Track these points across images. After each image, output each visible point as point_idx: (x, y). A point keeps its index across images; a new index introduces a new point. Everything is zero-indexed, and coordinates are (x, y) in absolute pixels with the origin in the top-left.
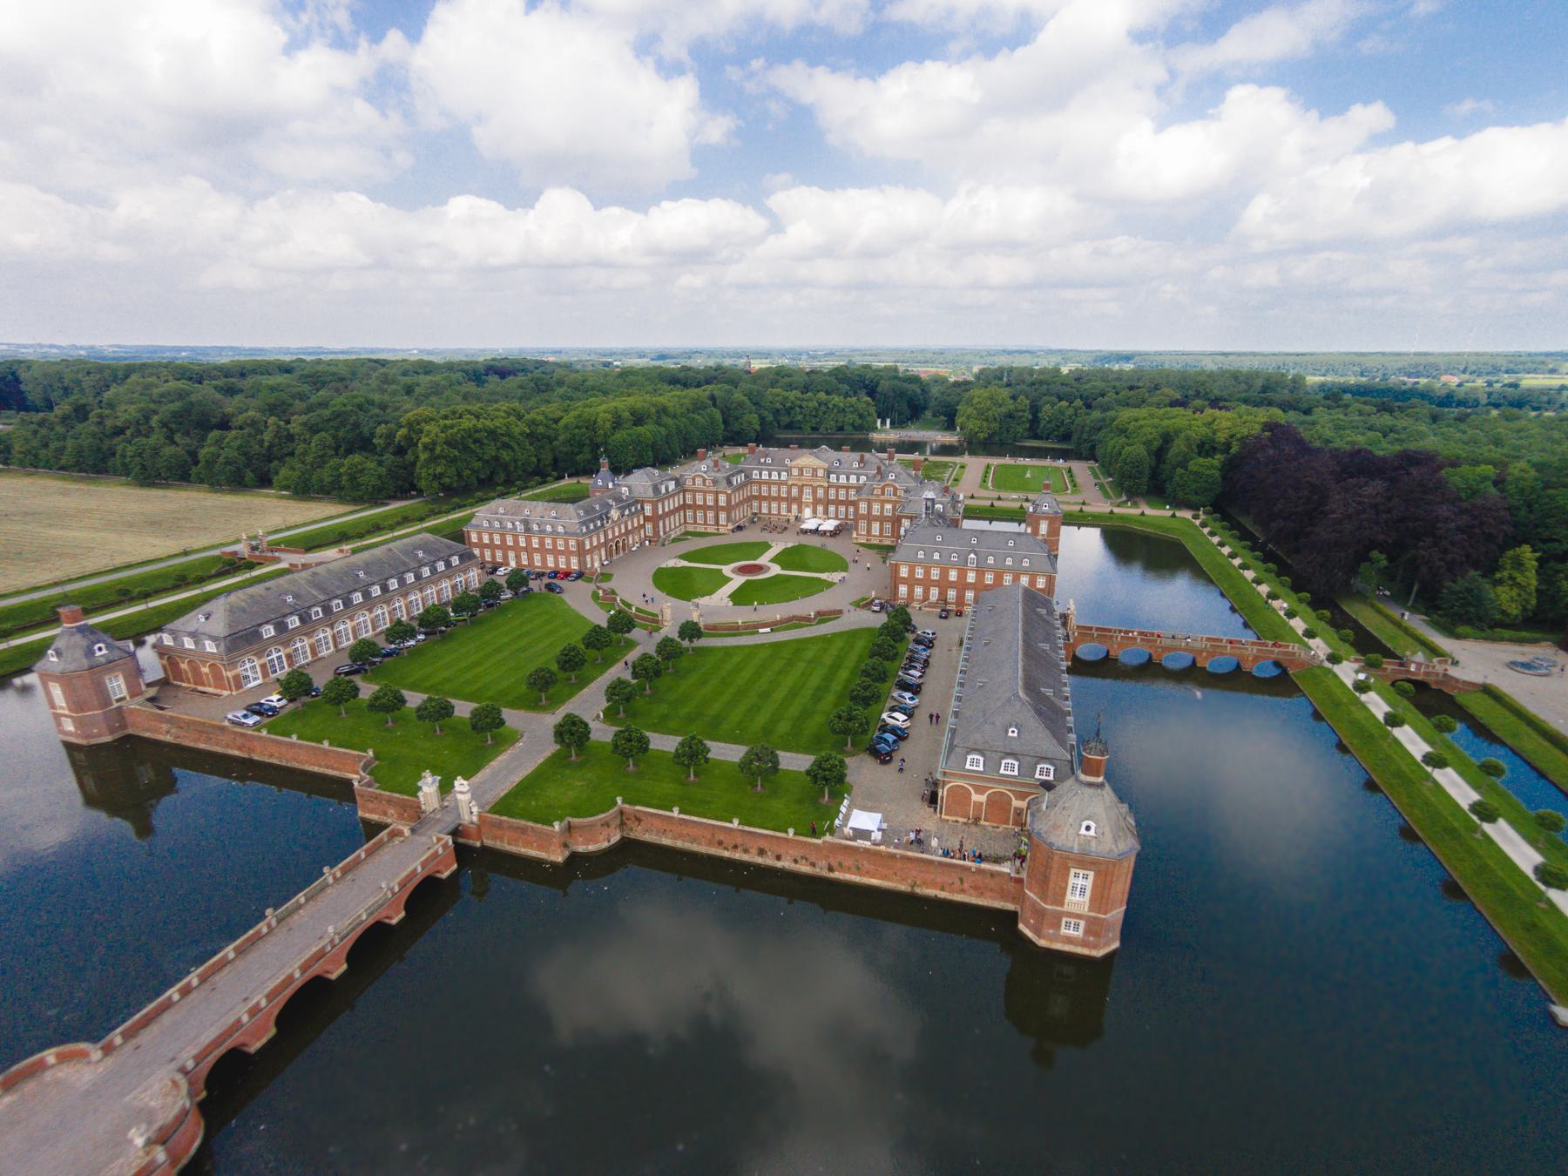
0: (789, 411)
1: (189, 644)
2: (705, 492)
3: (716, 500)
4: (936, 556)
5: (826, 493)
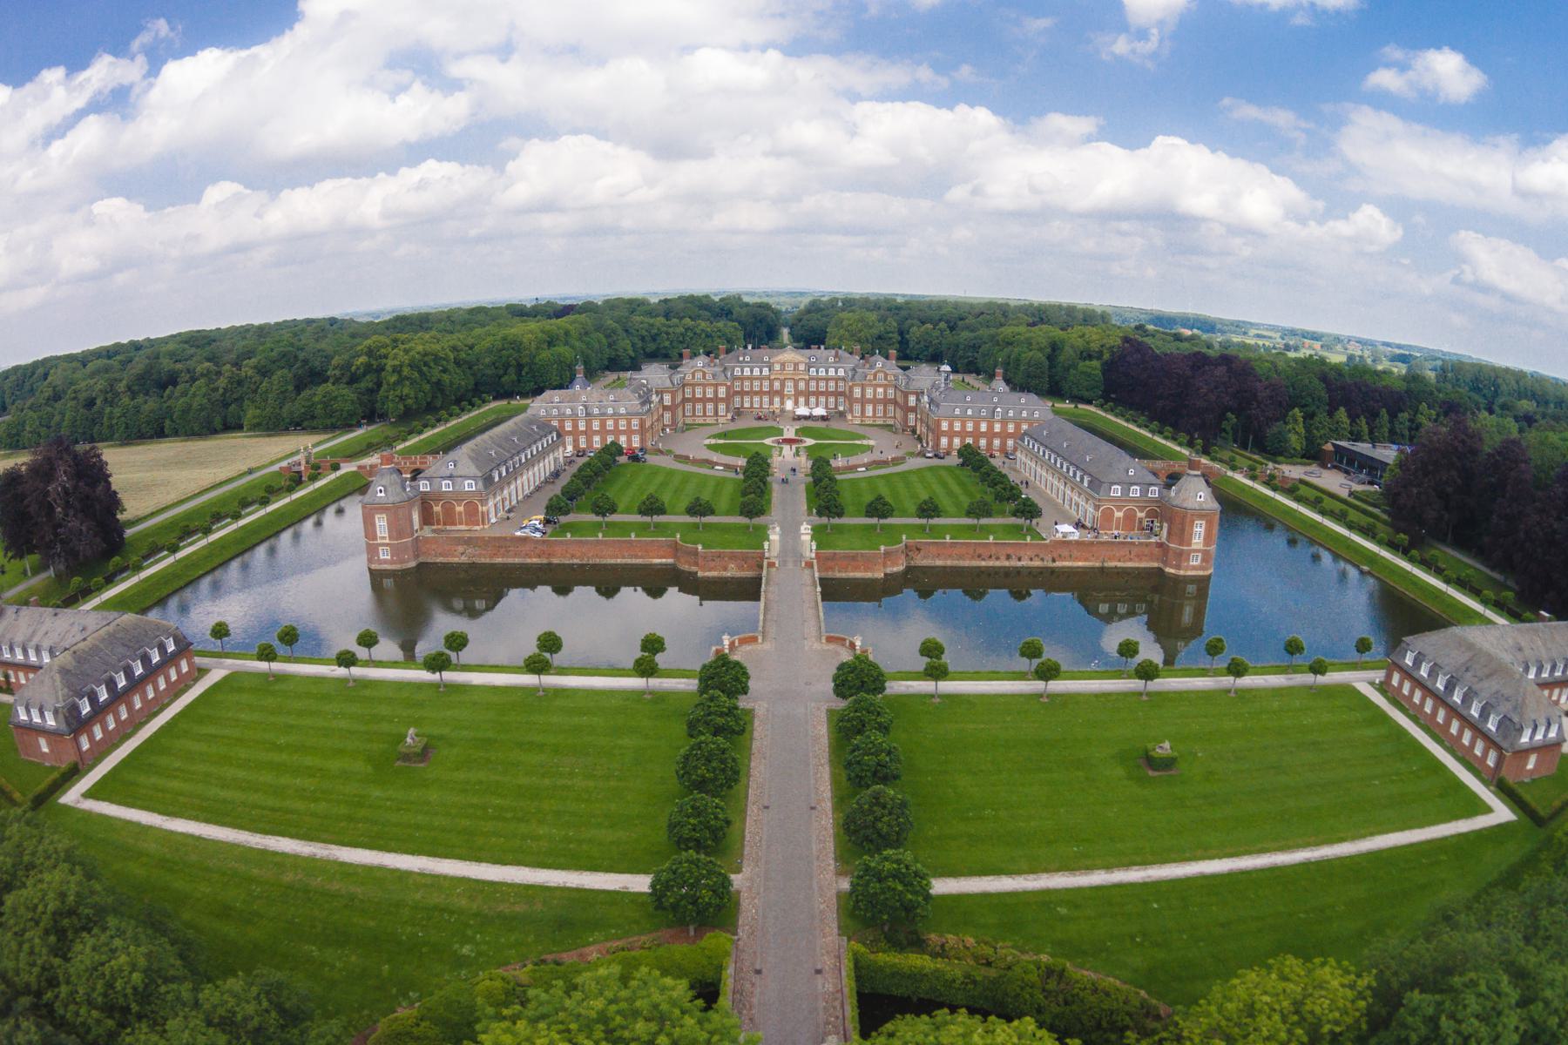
0: (654, 339)
1: (446, 486)
2: (704, 386)
3: (716, 392)
4: (970, 412)
5: (807, 385)
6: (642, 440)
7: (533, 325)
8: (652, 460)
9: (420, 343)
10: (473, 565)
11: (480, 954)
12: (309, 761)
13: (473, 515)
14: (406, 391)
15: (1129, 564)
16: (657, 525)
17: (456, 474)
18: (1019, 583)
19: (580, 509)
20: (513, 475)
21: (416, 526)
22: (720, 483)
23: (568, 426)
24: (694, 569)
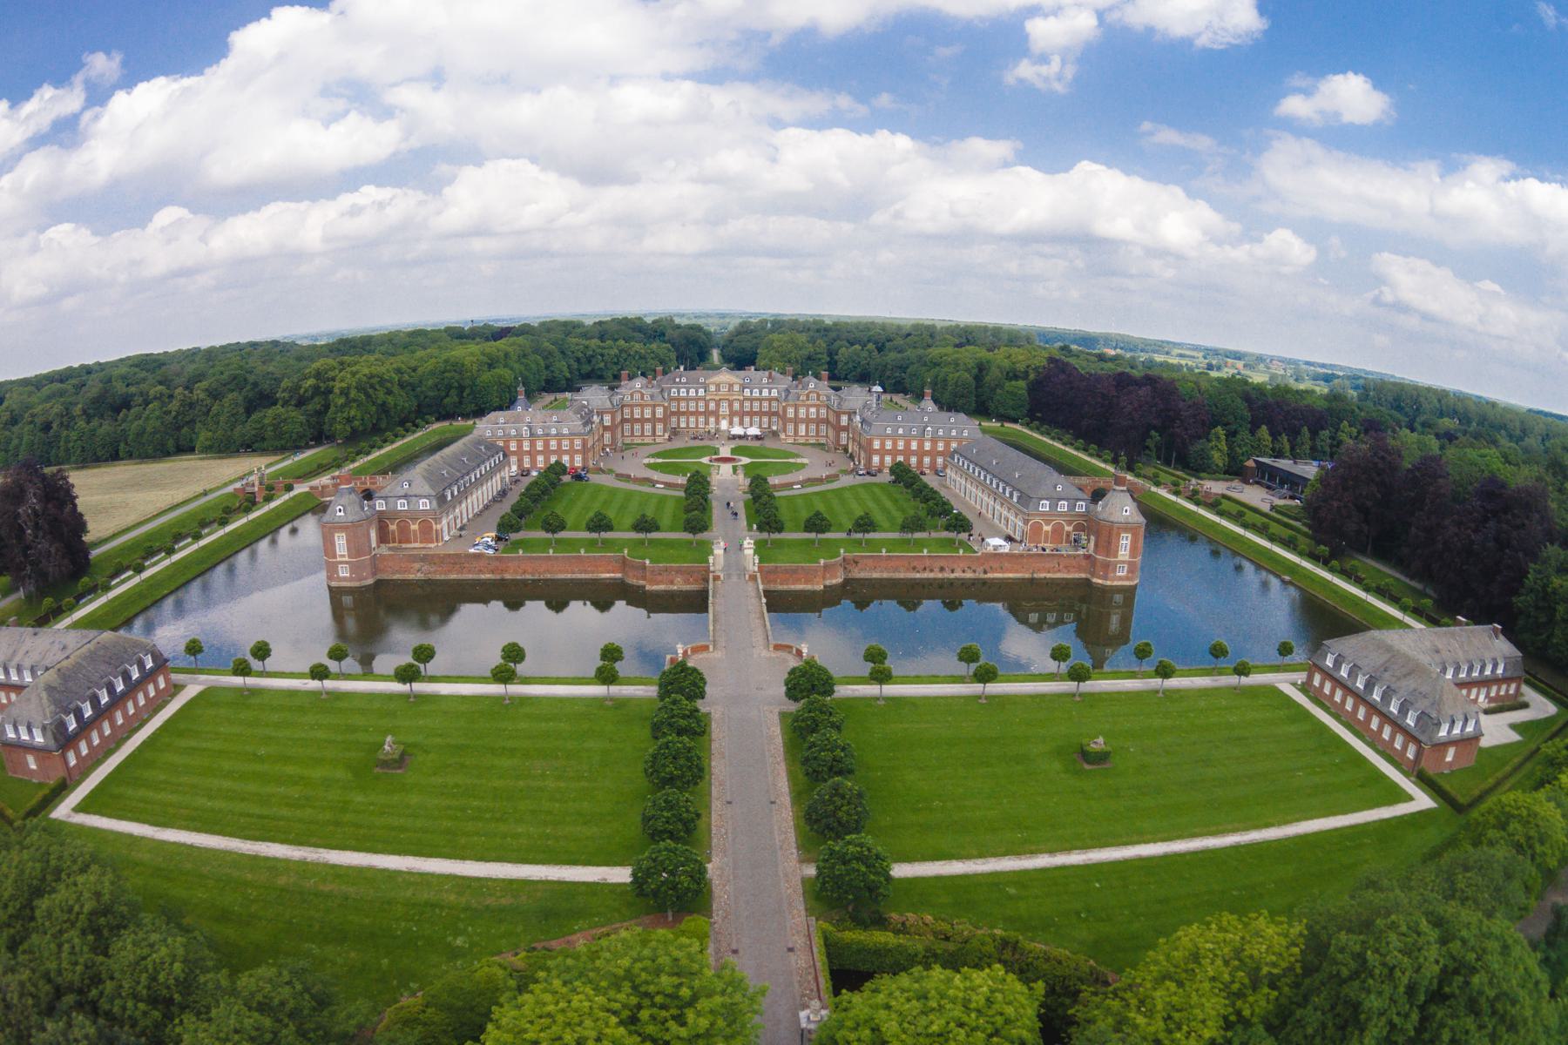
1: (402, 505)
3: (654, 413)
4: (901, 431)
5: (742, 406)
6: (585, 460)
7: (473, 347)
8: (595, 478)
9: (366, 366)
10: (428, 582)
11: (472, 945)
12: (290, 770)
13: (427, 533)
14: (353, 413)
15: (1058, 575)
16: (605, 542)
17: (409, 492)
18: (952, 594)
19: (529, 527)
20: (464, 494)
21: (374, 545)
22: (662, 500)
23: (513, 446)
24: (642, 582)
